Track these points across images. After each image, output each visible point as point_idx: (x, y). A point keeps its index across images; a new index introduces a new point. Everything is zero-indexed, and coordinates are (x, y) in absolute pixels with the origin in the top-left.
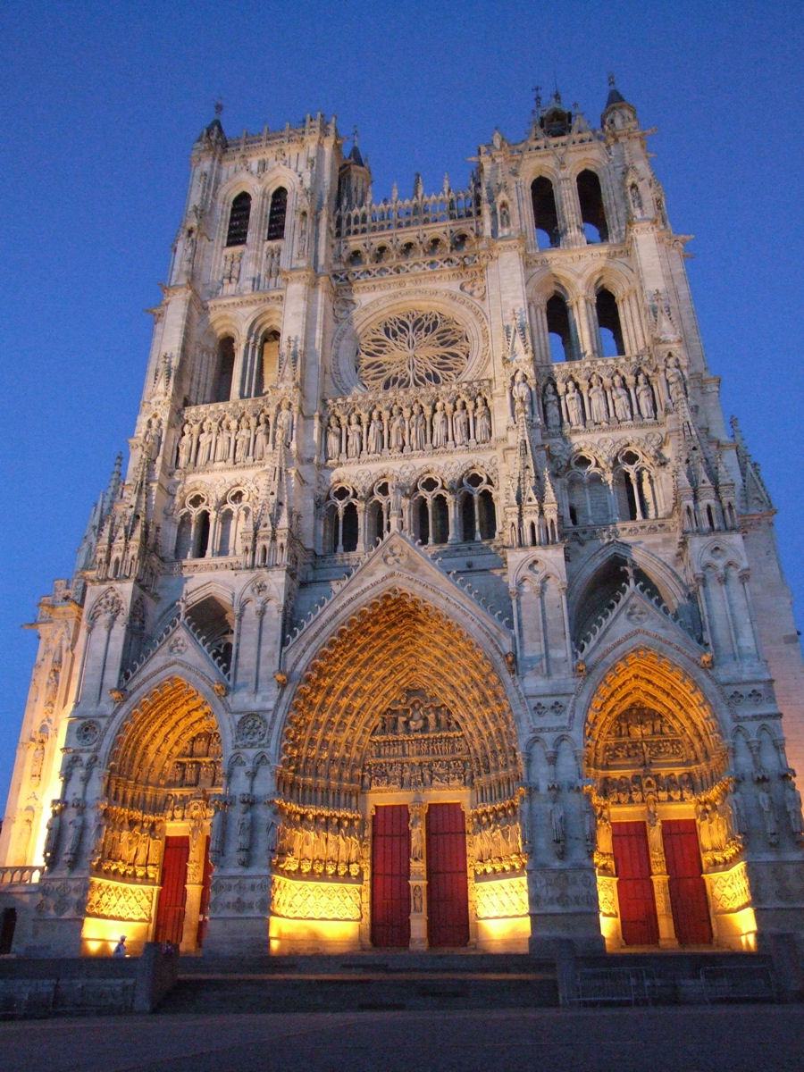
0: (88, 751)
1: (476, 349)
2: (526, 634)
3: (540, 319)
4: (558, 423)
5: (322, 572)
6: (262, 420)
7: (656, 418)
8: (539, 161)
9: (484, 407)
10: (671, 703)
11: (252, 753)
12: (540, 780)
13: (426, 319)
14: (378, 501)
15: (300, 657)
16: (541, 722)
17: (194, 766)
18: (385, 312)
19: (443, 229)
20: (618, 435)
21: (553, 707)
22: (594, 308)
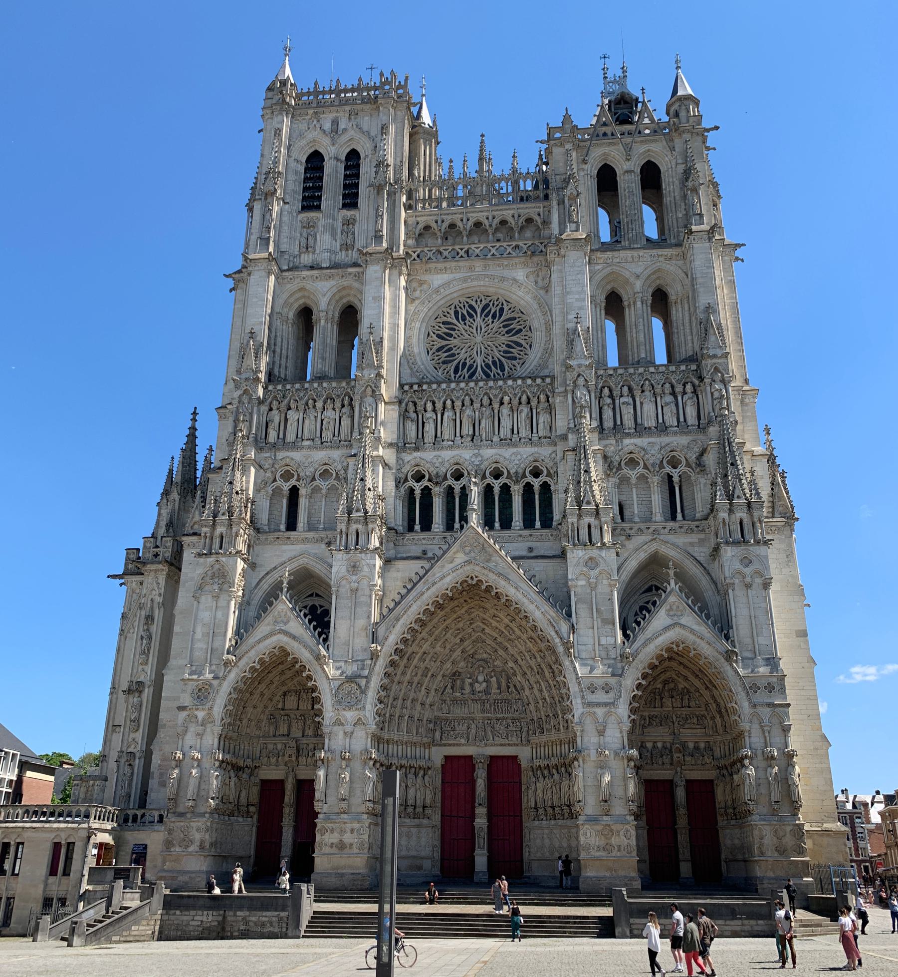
0: (203, 709)
3: (598, 316)
5: (401, 549)
6: (346, 402)
7: (699, 426)
8: (606, 150)
9: (546, 404)
10: (698, 682)
12: (592, 748)
13: (493, 304)
14: (450, 486)
17: (286, 718)
18: (455, 295)
19: (511, 212)
20: (665, 440)
22: (649, 308)
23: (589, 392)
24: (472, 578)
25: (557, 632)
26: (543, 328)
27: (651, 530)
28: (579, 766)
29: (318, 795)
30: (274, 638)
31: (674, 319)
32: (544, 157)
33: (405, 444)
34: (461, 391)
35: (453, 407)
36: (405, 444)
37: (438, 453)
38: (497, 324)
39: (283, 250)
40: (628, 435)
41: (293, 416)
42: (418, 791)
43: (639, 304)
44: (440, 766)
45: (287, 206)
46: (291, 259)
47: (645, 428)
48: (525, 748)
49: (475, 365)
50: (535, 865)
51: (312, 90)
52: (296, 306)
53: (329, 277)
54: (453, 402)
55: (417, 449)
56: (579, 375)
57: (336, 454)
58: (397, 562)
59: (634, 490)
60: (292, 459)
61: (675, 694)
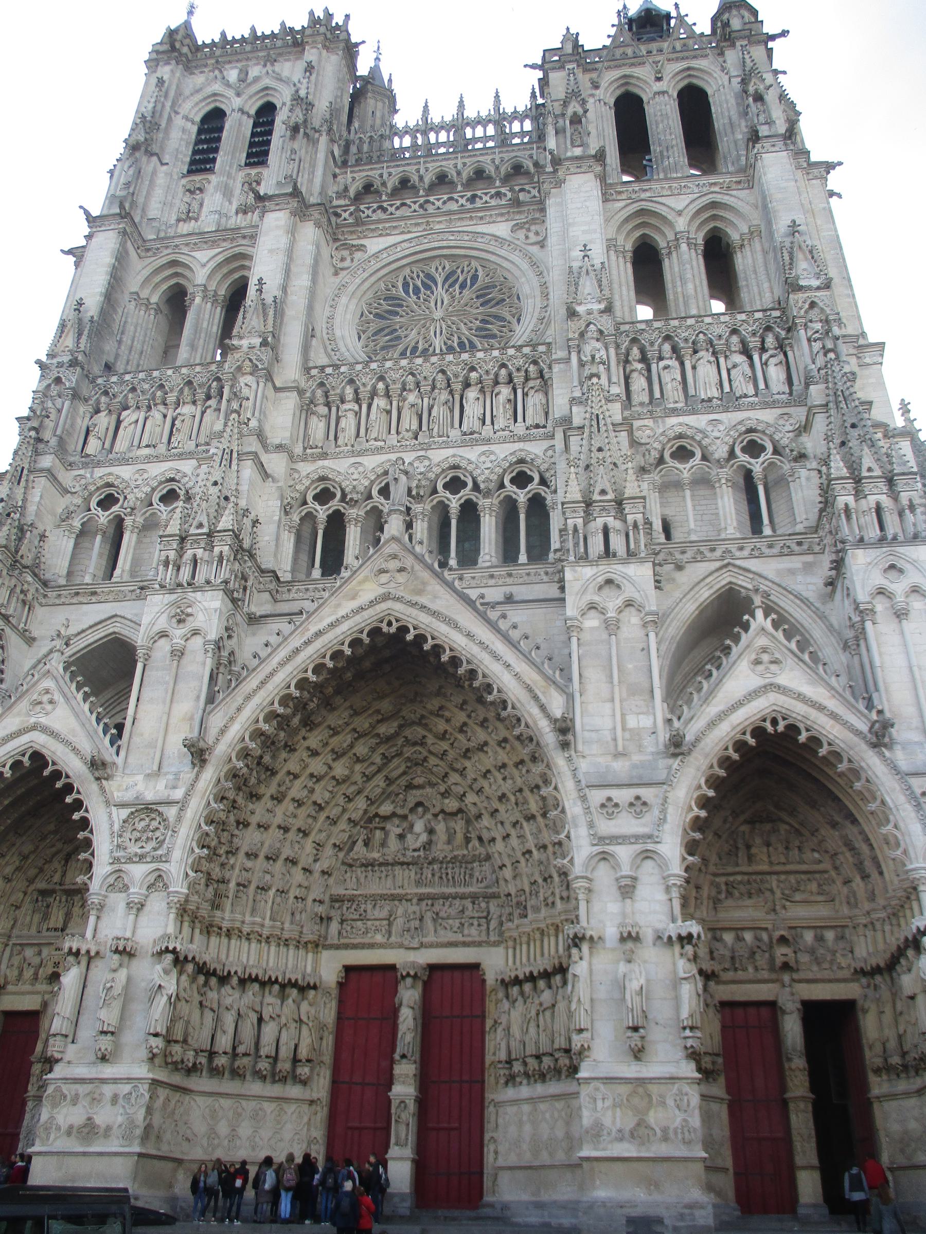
1: (531, 310)
2: (591, 688)
3: (622, 268)
4: (646, 399)
7: (791, 394)
11: (138, 872)
12: (608, 924)
13: (462, 272)
15: (232, 719)
16: (606, 827)
21: (631, 804)
24: (390, 624)
25: (543, 708)
26: (538, 293)
27: (718, 553)
28: (581, 959)
29: (57, 1025)
30: (24, 739)
31: (741, 268)
32: (538, 94)
36: (305, 449)
37: (358, 459)
40: (674, 412)
41: (129, 416)
42: (284, 1030)
43: (684, 247)
44: (333, 985)
45: (165, 167)
46: (164, 227)
47: (703, 401)
48: (493, 949)
50: (505, 1179)
52: (165, 287)
53: (214, 244)
55: (324, 456)
56: (588, 325)
57: (187, 466)
58: (270, 620)
59: (688, 493)
60: (118, 477)
61: (773, 839)
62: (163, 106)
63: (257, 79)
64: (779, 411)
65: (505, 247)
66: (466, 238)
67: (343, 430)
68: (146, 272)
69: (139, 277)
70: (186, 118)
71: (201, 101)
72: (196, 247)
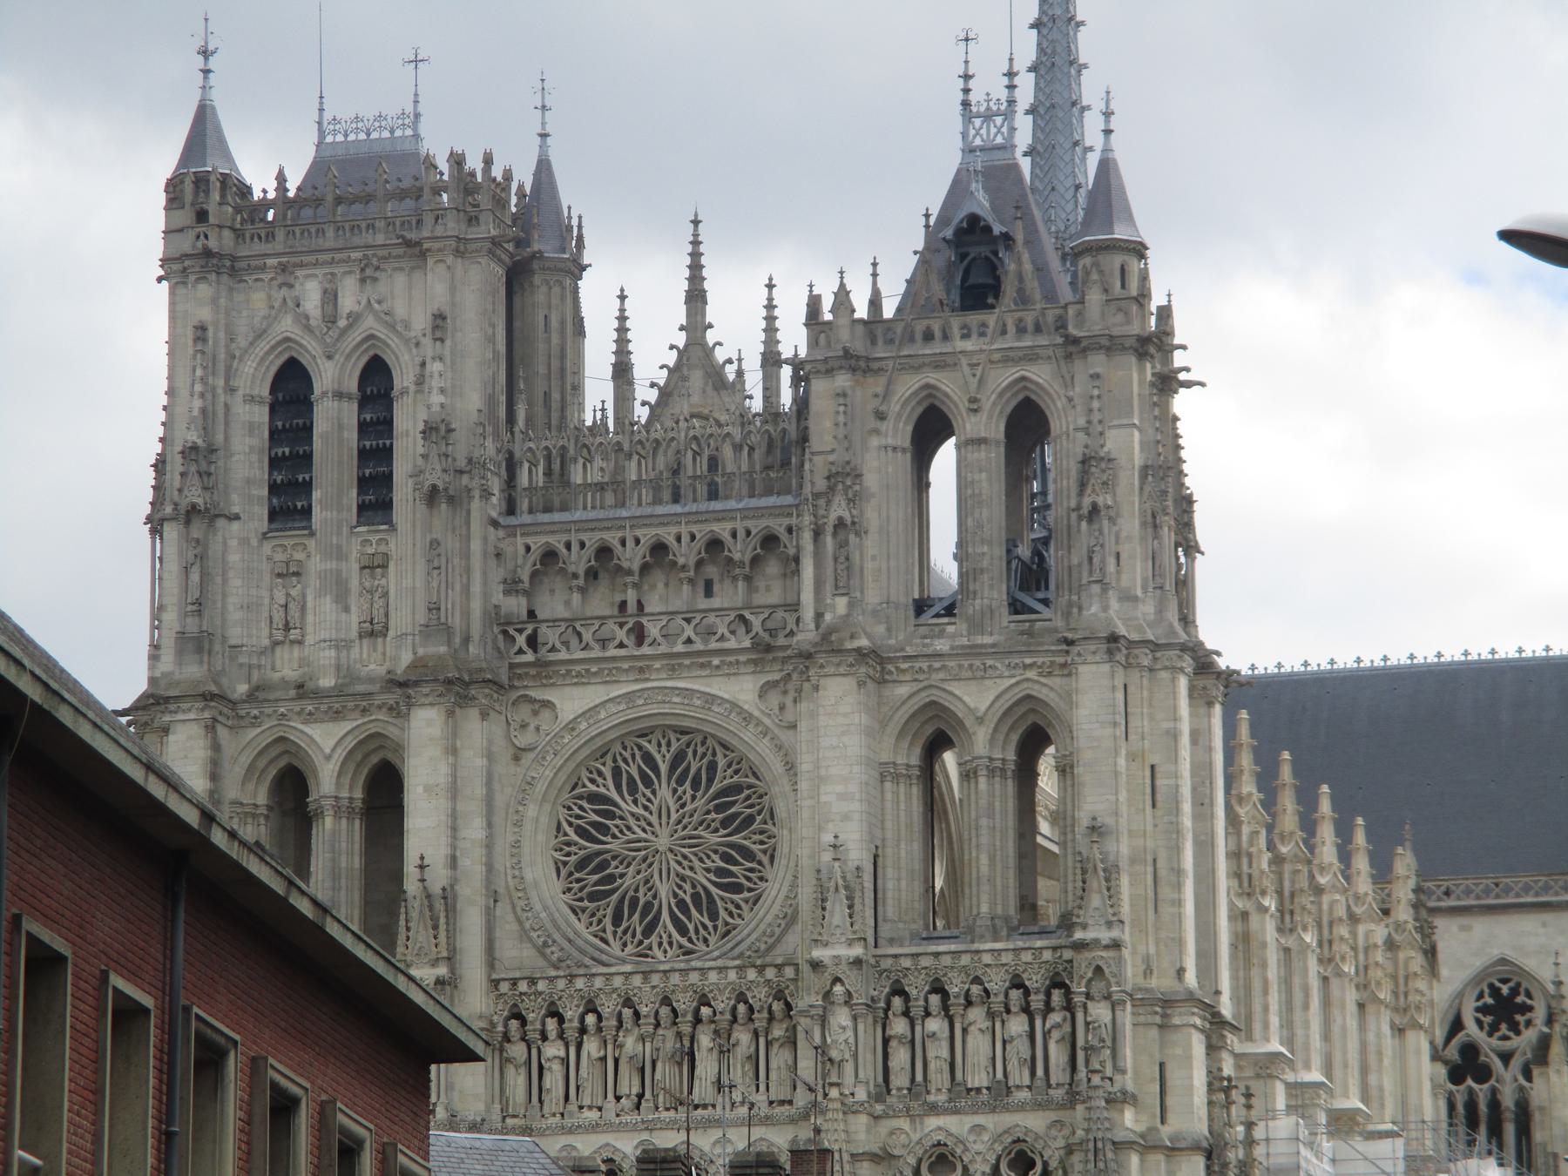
8: (932, 377)
18: (612, 735)
22: (1010, 782)
23: (855, 1018)
33: (504, 1118)
34: (615, 996)
35: (600, 1030)
36: (504, 1118)
38: (699, 803)
39: (233, 642)
40: (934, 1109)
45: (235, 526)
46: (254, 661)
47: (969, 1090)
49: (656, 903)
51: (271, 195)
52: (273, 772)
53: (338, 715)
54: (600, 1018)
62: (214, 389)
63: (354, 318)
64: (1052, 1116)
65: (751, 727)
66: (698, 703)
67: (549, 1091)
68: (245, 760)
69: (237, 769)
70: (251, 399)
71: (268, 353)
72: (310, 718)
